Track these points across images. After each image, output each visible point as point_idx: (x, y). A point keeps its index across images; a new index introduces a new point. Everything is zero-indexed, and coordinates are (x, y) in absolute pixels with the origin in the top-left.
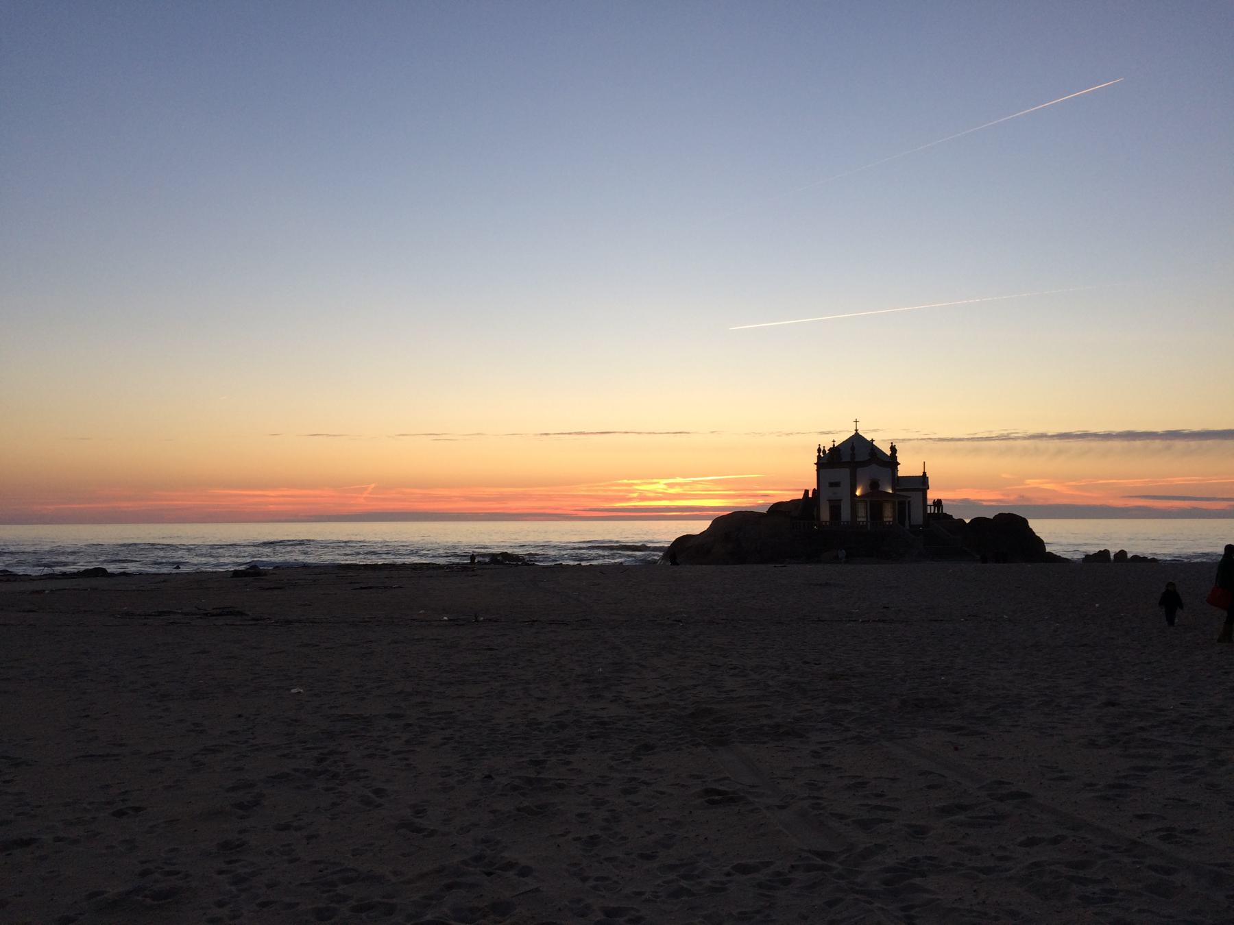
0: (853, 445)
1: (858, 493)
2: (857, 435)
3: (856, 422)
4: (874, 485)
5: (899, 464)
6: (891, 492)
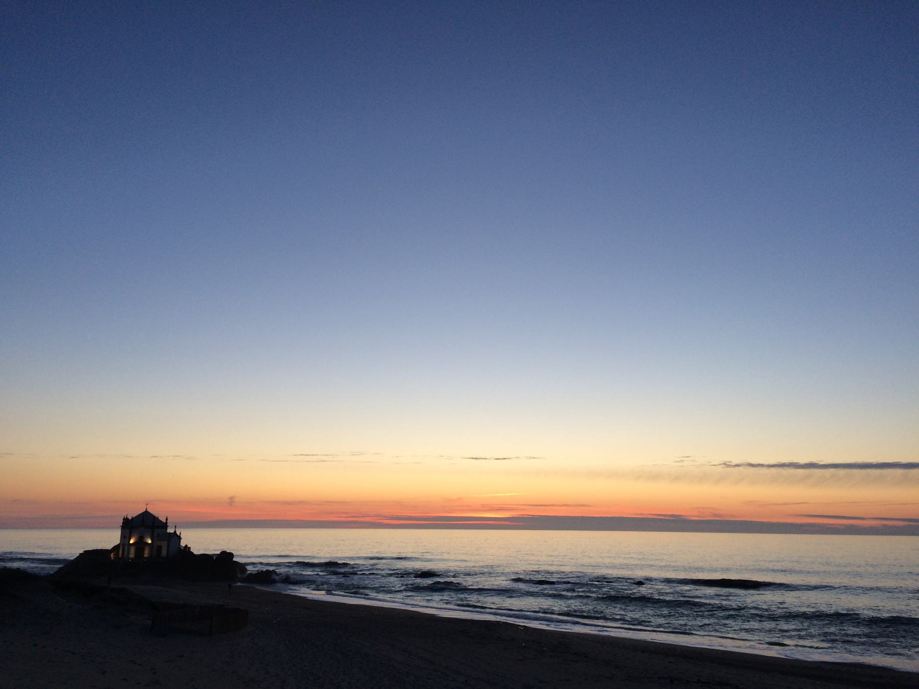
1: (132, 542)
2: (146, 511)
6: (150, 542)
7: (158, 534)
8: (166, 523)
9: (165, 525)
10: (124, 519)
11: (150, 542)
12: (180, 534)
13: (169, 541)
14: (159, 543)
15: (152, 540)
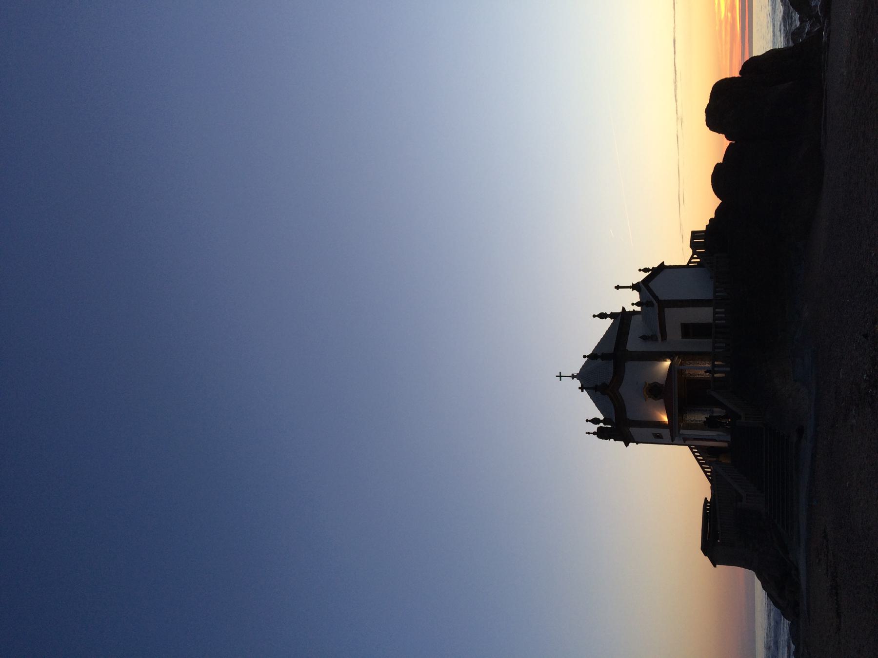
0: (590, 421)
2: (578, 376)
3: (560, 376)
4: (656, 391)
5: (624, 309)
6: (667, 363)
7: (644, 338)
8: (613, 315)
9: (622, 319)
10: (602, 434)
11: (667, 363)
12: (645, 270)
13: (664, 305)
14: (674, 333)
15: (662, 357)
